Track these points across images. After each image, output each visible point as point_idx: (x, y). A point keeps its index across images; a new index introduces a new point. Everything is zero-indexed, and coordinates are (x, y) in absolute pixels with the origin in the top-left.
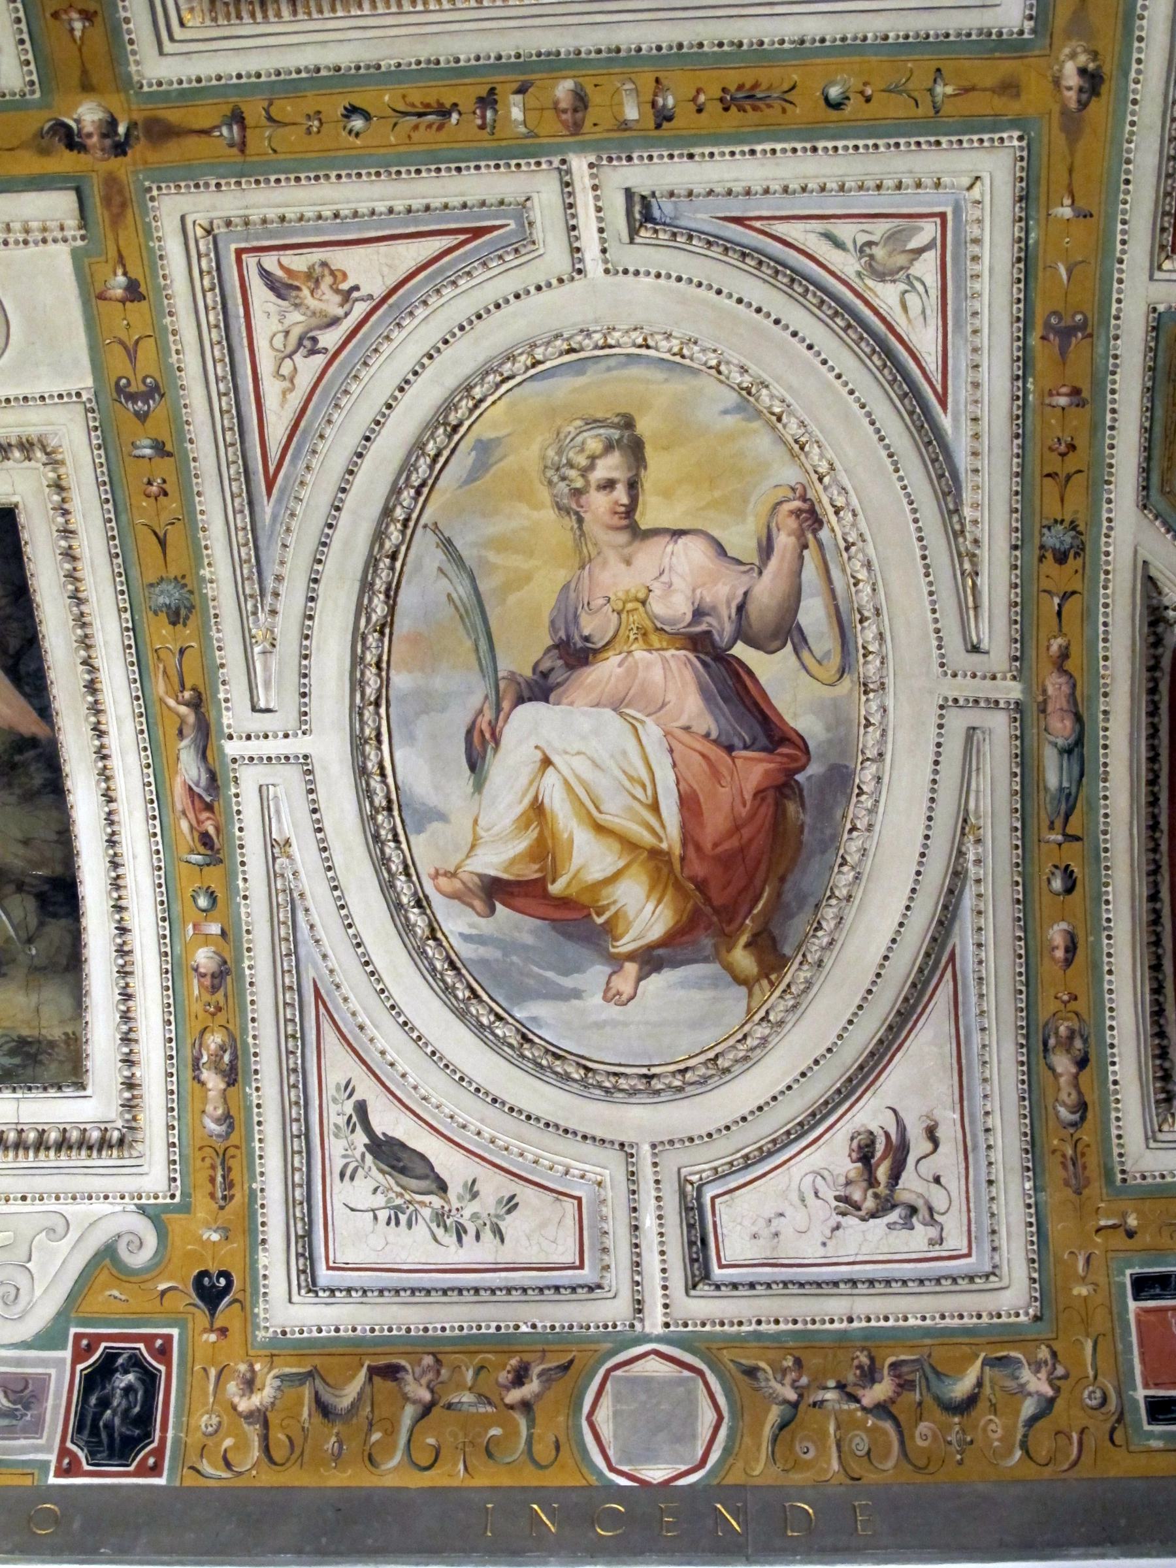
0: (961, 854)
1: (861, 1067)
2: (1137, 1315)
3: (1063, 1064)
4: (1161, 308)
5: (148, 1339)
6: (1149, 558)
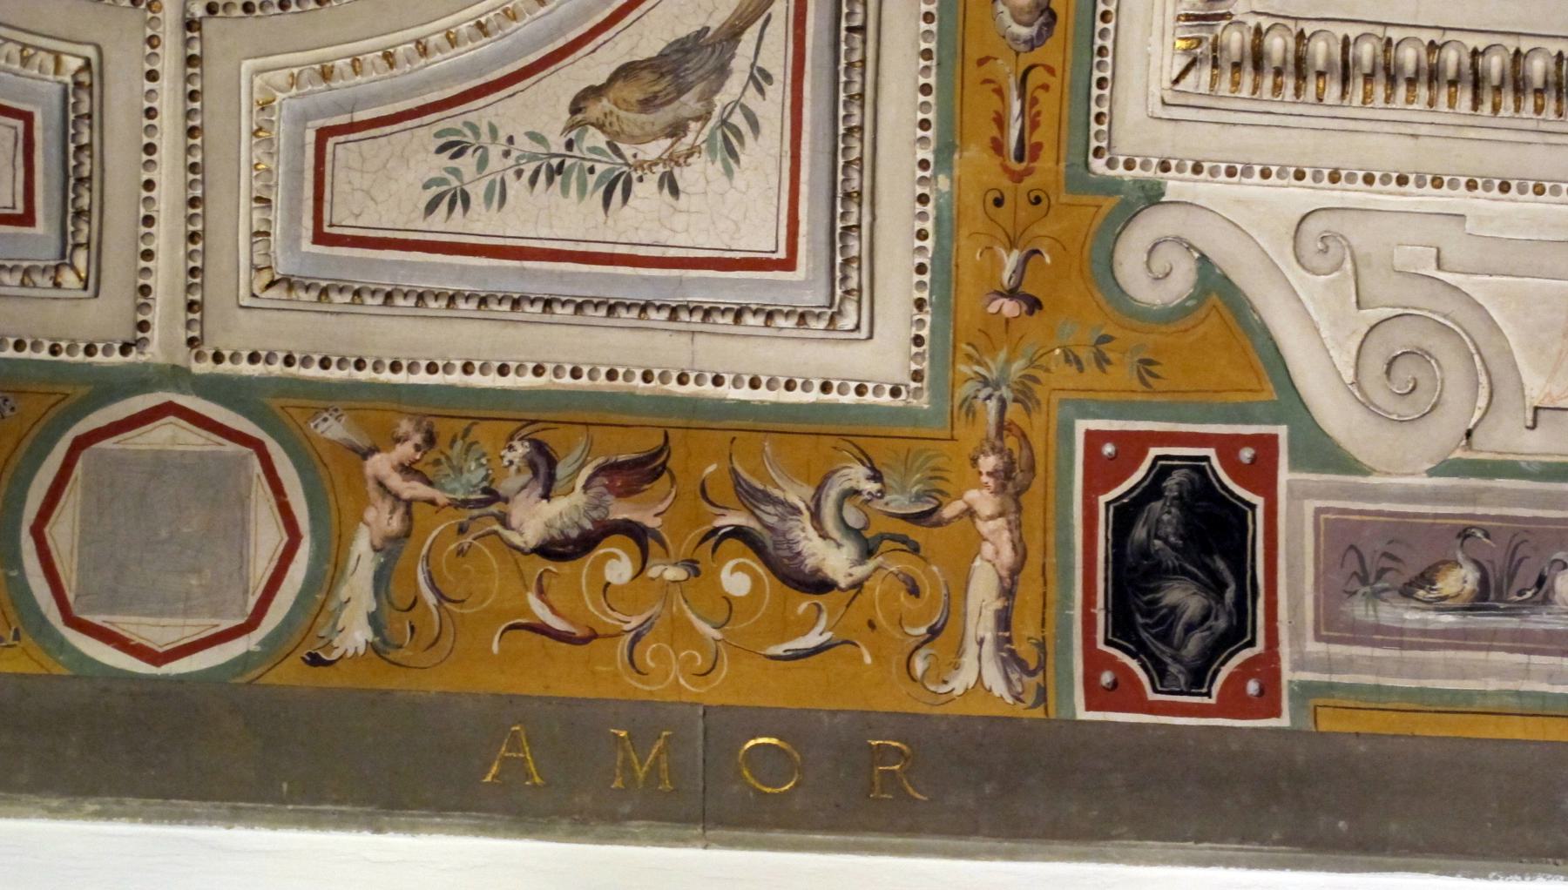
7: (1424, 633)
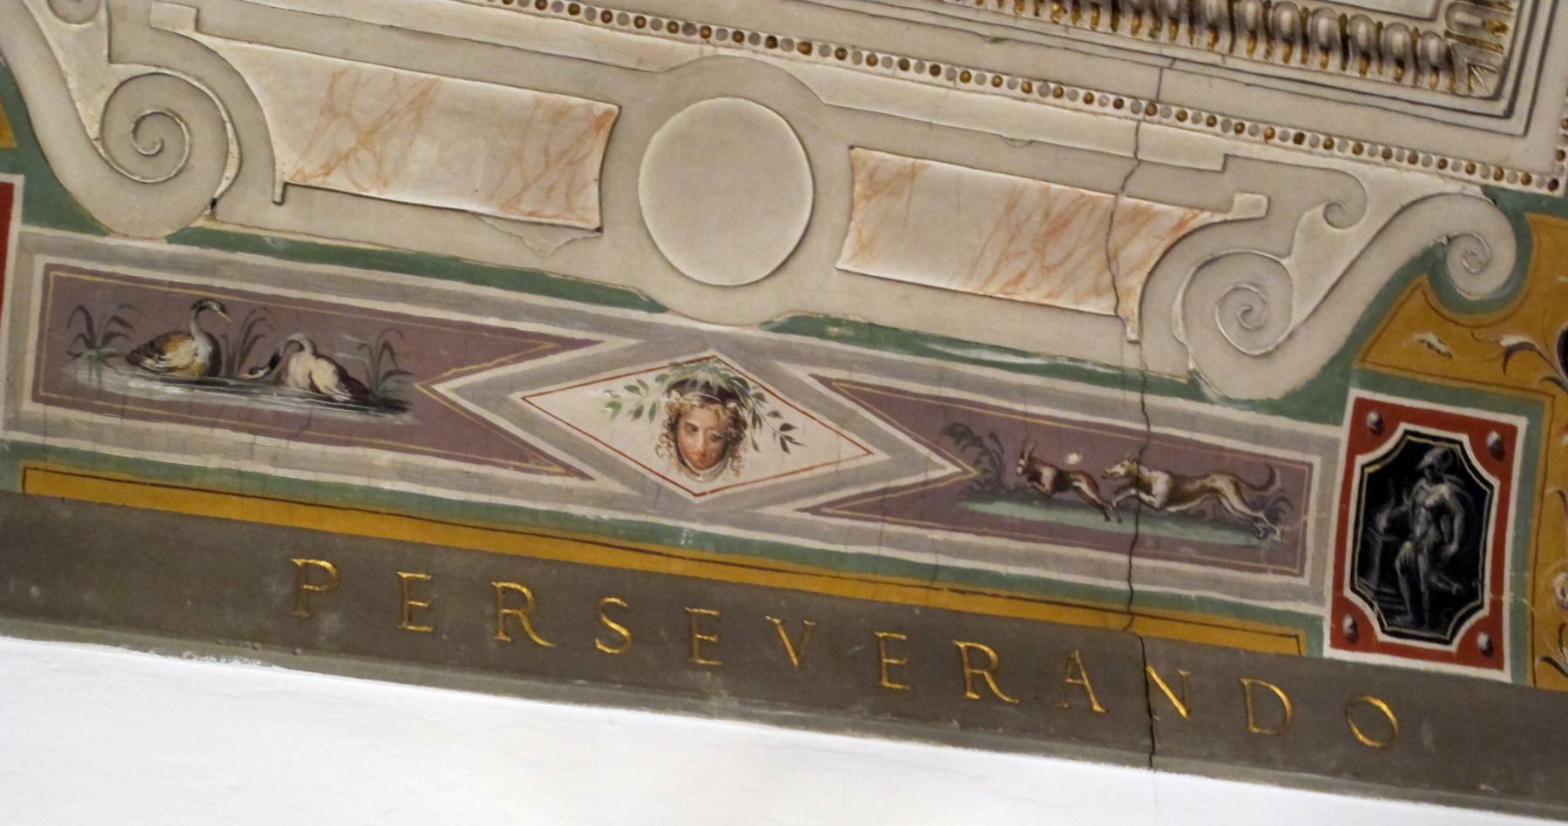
5: (1478, 429)
7: (151, 403)
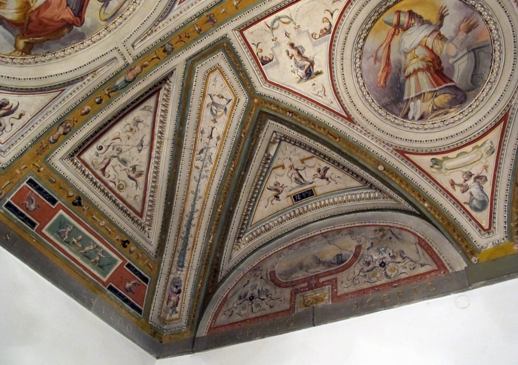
0: (87, 75)
1: (22, 89)
2: (24, 186)
3: (61, 130)
4: (228, 36)
6: (177, 69)
